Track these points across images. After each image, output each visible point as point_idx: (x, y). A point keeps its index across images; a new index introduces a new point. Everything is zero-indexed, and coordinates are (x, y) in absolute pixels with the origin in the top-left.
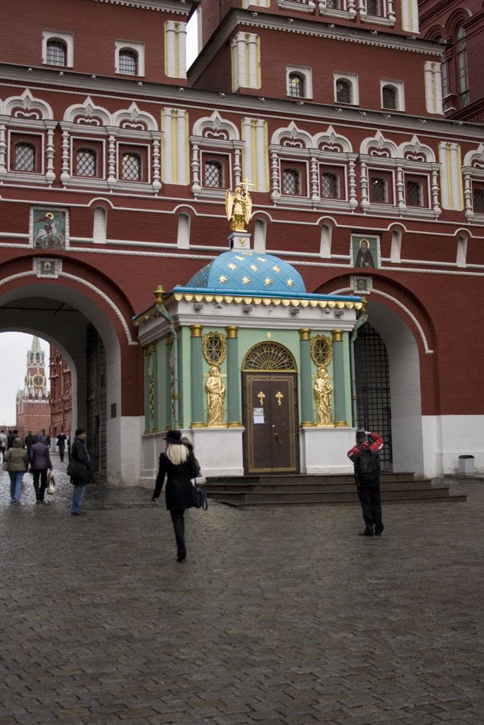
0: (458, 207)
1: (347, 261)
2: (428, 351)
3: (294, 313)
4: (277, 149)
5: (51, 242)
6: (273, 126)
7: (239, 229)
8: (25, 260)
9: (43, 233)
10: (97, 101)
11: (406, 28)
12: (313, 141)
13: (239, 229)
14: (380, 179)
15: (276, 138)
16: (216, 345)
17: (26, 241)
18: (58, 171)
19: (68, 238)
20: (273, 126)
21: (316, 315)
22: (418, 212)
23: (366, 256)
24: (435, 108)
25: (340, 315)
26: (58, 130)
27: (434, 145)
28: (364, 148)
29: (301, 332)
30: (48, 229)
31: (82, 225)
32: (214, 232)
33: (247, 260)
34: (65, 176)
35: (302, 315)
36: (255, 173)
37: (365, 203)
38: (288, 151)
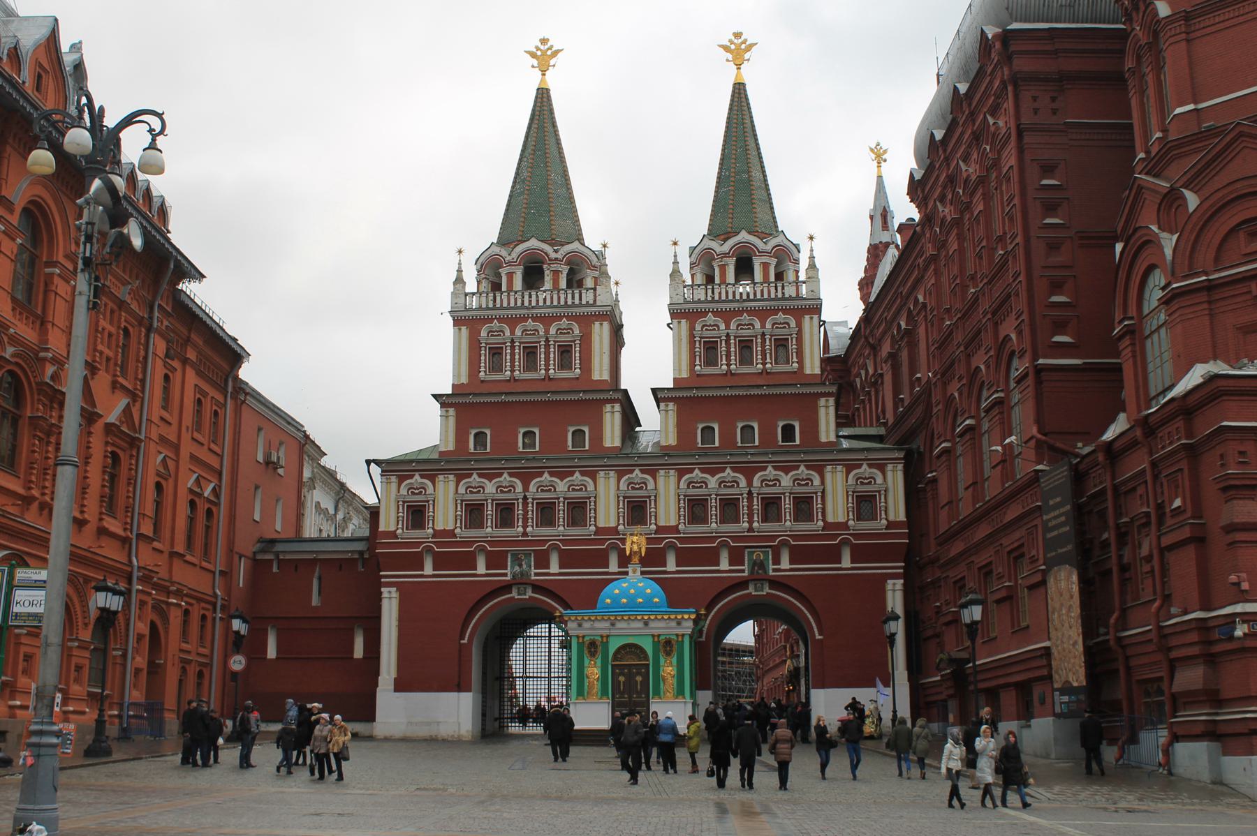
0: (841, 519)
1: (743, 571)
2: (818, 637)
3: (646, 624)
4: (682, 492)
5: (522, 574)
6: (681, 474)
7: (636, 560)
8: (507, 588)
9: (517, 568)
10: (552, 474)
11: (808, 371)
12: (713, 482)
13: (636, 560)
14: (771, 506)
15: (683, 485)
16: (592, 647)
17: (505, 575)
18: (525, 526)
19: (533, 571)
20: (681, 474)
21: (662, 624)
22: (804, 527)
23: (762, 565)
24: (828, 436)
25: (682, 624)
26: (525, 498)
27: (820, 471)
28: (756, 482)
29: (653, 636)
30: (520, 566)
31: (543, 561)
32: (624, 561)
33: (634, 586)
34: (529, 529)
35: (652, 625)
36: (668, 509)
37: (755, 525)
38: (691, 491)
